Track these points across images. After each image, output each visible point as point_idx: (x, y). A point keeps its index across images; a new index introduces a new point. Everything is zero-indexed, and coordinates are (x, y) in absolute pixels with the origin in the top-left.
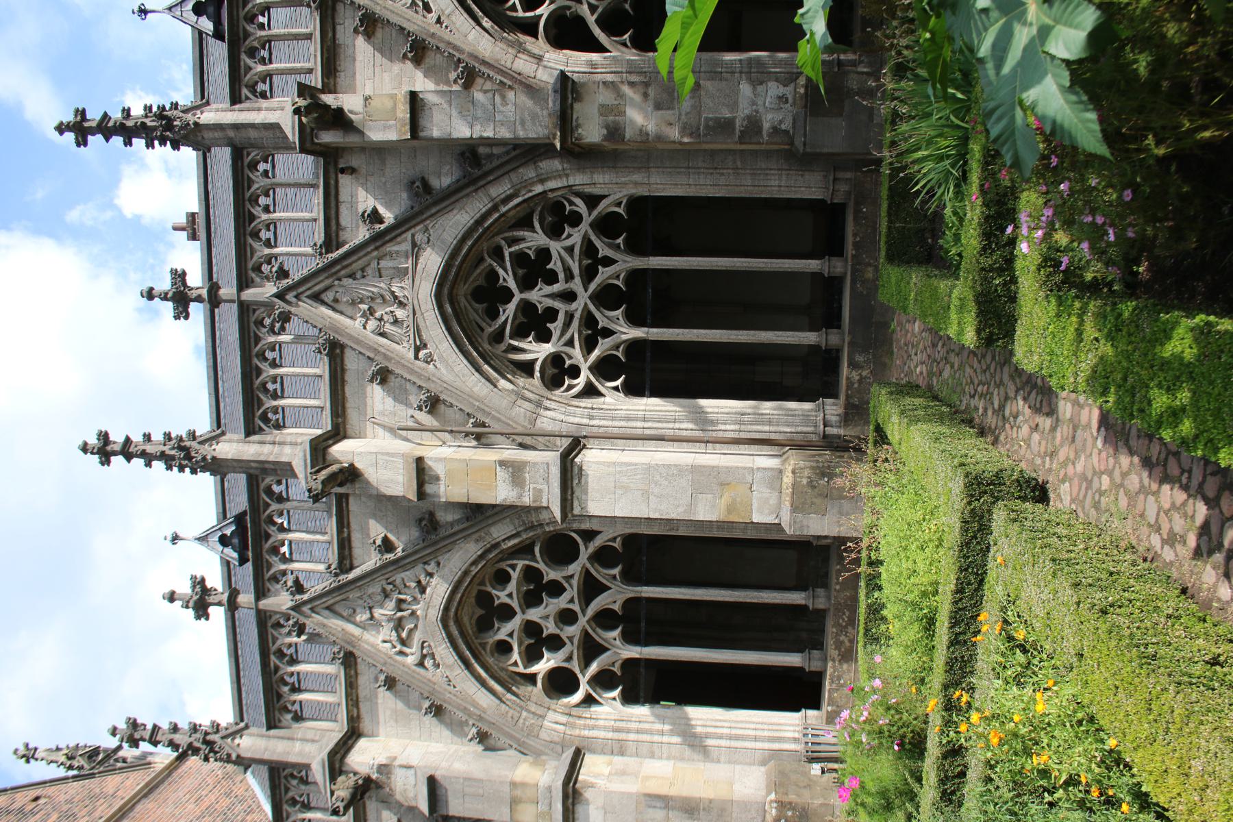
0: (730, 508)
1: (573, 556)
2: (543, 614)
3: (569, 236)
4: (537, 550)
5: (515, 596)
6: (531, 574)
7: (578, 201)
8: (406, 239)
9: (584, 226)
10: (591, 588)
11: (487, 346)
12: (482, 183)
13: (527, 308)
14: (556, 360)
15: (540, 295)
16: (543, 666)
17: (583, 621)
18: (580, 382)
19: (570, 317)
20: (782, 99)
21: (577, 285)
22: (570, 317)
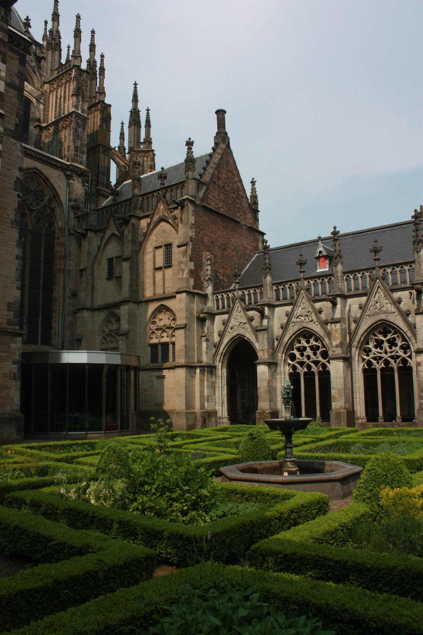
0: (335, 398)
1: (324, 358)
2: (309, 352)
4: (324, 349)
6: (318, 348)
7: (409, 353)
10: (316, 363)
13: (382, 342)
14: (370, 350)
16: (295, 352)
17: (308, 362)
18: (365, 357)
19: (381, 353)
22: (381, 353)
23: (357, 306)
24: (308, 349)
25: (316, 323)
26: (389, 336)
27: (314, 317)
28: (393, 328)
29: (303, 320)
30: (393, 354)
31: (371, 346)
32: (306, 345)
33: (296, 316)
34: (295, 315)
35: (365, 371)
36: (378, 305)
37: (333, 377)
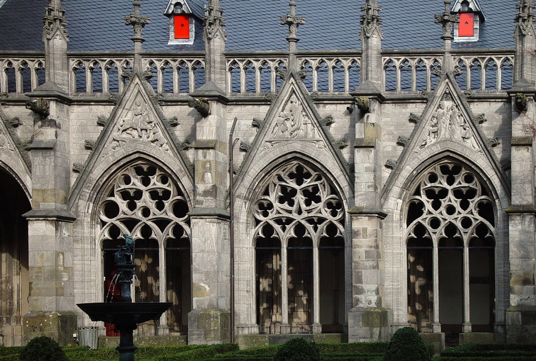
2: (146, 200)
3: (326, 211)
5: (155, 187)
6: (167, 194)
7: (341, 216)
8: (320, 137)
9: (330, 218)
11: (275, 173)
12: (345, 173)
13: (294, 192)
14: (270, 206)
15: (300, 198)
16: (117, 199)
17: (144, 220)
18: (260, 217)
19: (290, 212)
20: (370, 302)
21: (305, 215)
22: (290, 212)
23: (250, 122)
24: (146, 196)
25: (164, 145)
26: (307, 183)
27: (160, 134)
28: (315, 169)
29: (137, 137)
30: (310, 215)
31: (272, 197)
32: (140, 186)
33: (122, 129)
34: (118, 126)
35: (258, 242)
36: (288, 124)
37: (197, 250)
